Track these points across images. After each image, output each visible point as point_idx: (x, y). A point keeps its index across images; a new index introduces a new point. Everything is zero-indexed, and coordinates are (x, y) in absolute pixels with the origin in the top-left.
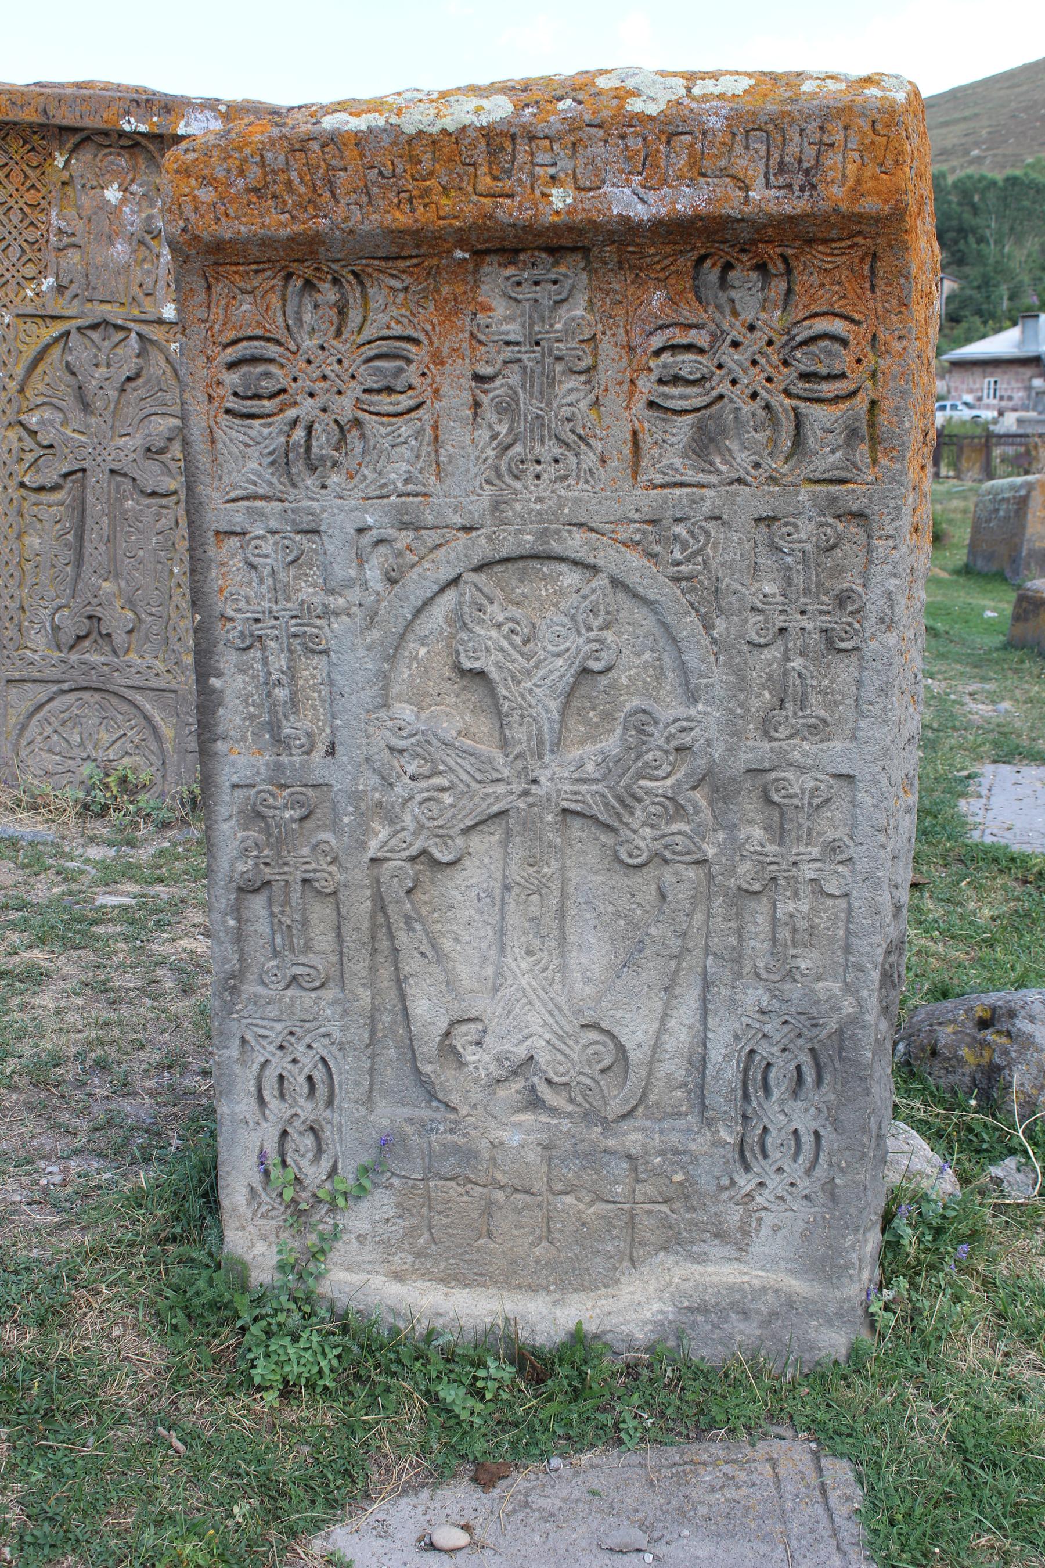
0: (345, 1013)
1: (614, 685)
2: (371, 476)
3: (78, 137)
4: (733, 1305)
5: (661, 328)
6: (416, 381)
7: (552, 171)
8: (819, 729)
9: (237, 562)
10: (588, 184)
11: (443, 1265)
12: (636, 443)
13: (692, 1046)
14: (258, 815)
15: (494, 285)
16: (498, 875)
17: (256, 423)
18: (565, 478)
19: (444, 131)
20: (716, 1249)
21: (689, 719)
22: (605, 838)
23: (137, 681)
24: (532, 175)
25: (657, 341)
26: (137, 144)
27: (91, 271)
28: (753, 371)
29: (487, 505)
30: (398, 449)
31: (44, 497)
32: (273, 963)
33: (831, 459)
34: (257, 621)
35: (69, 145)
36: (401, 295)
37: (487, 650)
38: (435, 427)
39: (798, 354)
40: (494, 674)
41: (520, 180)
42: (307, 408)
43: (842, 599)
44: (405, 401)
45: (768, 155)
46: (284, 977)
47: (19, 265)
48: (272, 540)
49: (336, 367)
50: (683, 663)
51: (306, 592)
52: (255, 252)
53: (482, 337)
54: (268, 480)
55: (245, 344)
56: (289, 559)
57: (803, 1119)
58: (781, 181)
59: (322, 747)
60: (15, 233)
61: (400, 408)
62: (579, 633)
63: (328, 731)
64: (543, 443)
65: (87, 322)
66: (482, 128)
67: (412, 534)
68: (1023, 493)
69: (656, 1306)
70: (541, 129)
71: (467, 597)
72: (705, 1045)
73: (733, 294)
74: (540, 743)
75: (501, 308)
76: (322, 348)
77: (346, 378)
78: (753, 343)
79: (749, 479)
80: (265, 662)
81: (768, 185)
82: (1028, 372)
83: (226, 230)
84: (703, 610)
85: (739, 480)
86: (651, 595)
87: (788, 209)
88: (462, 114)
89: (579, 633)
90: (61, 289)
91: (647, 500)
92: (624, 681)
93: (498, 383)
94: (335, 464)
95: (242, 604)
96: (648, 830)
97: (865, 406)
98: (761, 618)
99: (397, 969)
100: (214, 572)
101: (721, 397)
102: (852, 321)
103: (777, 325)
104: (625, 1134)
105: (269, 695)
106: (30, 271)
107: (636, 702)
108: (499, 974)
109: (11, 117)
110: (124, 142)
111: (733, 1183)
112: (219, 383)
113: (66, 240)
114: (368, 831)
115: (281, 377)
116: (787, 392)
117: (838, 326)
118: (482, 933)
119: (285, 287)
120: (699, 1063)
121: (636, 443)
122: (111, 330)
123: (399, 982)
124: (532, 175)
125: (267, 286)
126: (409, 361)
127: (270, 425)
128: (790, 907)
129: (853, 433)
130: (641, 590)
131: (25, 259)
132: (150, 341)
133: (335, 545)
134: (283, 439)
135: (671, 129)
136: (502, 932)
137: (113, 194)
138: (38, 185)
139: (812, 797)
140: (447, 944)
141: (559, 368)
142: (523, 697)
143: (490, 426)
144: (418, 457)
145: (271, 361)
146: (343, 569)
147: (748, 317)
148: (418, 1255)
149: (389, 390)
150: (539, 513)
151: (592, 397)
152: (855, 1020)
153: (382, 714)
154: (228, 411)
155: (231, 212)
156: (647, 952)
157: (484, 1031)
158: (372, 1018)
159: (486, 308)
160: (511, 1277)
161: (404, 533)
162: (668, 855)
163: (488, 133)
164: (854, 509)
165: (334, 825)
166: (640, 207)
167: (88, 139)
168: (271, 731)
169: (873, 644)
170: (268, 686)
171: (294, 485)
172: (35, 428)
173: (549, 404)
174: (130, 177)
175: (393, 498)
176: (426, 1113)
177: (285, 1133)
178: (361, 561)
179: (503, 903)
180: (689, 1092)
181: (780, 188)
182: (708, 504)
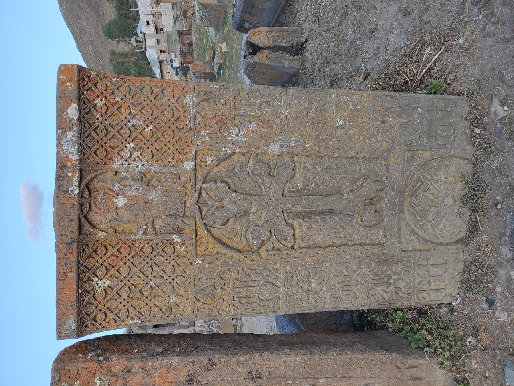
3: (85, 223)
26: (87, 186)
27: (167, 213)
31: (297, 234)
35: (91, 229)
47: (167, 257)
60: (147, 260)
65: (197, 214)
68: (201, 6)
82: (163, 65)
90: (180, 231)
106: (169, 250)
109: (74, 265)
110: (86, 194)
113: (150, 229)
122: (201, 200)
131: (162, 253)
132: (207, 176)
137: (121, 202)
138: (118, 246)
167: (85, 217)
172: (260, 241)
174: (108, 191)
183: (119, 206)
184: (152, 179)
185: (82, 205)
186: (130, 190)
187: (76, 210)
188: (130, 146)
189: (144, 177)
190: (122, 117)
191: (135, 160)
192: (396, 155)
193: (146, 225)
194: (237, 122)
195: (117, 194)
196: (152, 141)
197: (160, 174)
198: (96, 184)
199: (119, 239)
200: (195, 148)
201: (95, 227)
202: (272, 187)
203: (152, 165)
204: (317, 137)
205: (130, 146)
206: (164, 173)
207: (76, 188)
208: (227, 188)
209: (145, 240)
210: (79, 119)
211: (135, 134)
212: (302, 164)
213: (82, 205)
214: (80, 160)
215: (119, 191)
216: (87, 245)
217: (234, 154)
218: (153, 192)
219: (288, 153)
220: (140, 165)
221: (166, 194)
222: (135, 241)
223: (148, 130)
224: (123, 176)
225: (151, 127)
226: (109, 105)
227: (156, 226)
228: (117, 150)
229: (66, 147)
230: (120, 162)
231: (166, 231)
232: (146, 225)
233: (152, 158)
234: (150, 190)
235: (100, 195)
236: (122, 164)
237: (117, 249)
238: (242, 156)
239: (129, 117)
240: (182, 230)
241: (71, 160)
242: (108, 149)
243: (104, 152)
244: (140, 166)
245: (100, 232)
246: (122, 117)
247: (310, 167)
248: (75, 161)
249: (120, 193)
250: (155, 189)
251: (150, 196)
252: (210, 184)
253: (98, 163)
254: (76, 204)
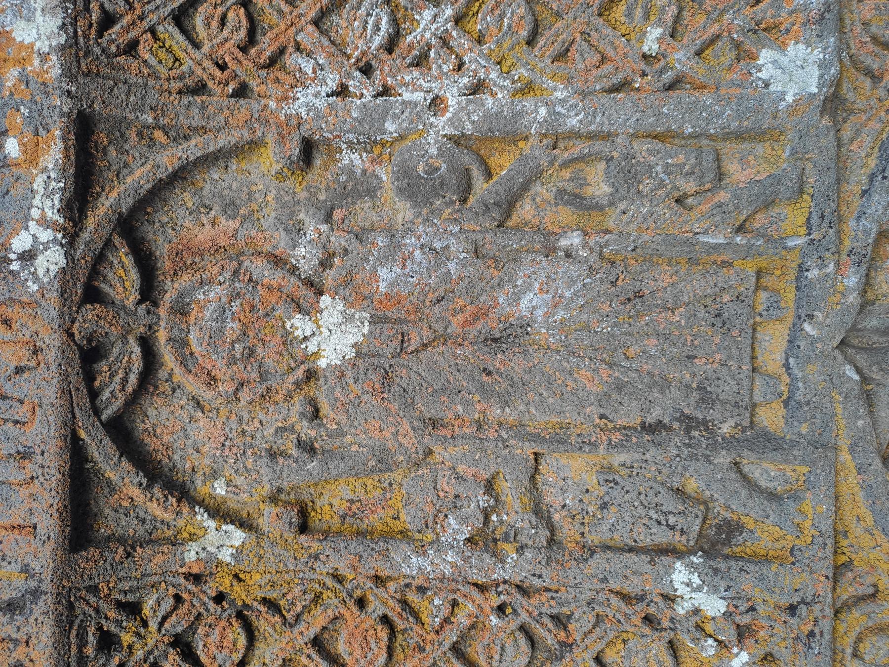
35: (157, 508)
110: (123, 279)
113: (514, 514)
137: (333, 335)
138: (318, 620)
174: (259, 268)
183: (322, 363)
184: (525, 187)
185: (90, 355)
186: (387, 257)
187: (44, 388)
189: (476, 173)
191: (420, 61)
193: (490, 486)
195: (309, 283)
197: (579, 148)
198: (183, 225)
199: (323, 569)
201: (181, 492)
203: (527, 88)
206: (607, 137)
207: (46, 235)
209: (482, 588)
213: (90, 355)
214: (75, 53)
215: (325, 264)
216: (133, 609)
218: (532, 270)
221: (622, 279)
222: (422, 590)
224: (350, 171)
227: (552, 498)
230: (332, 83)
231: (621, 537)
232: (490, 486)
233: (531, 42)
234: (515, 258)
235: (216, 293)
236: (342, 91)
237: (311, 633)
240: (731, 529)
244: (452, 101)
245: (211, 524)
248: (44, 57)
249: (330, 277)
250: (549, 251)
251: (517, 299)
253: (200, 88)
254: (52, 340)
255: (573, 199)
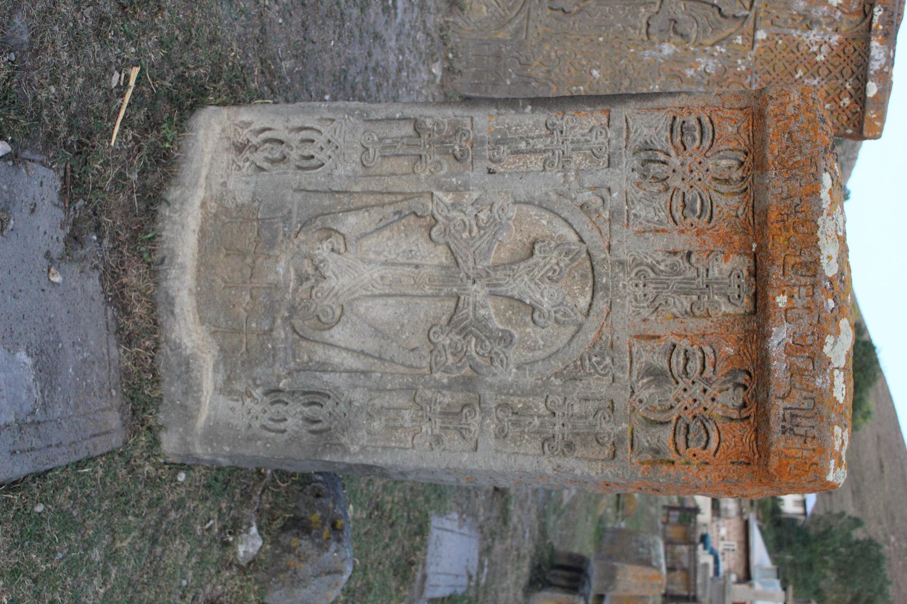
0: (349, 177)
1: (526, 324)
2: (638, 196)
4: (191, 386)
5: (714, 351)
6: (688, 221)
7: (796, 296)
8: (501, 434)
9: (594, 122)
10: (789, 315)
11: (210, 229)
12: (654, 337)
13: (332, 364)
14: (457, 131)
15: (739, 263)
16: (423, 262)
17: (668, 134)
18: (636, 300)
19: (818, 239)
20: (220, 378)
21: (507, 365)
22: (445, 319)
23: (533, 14)
24: (794, 285)
25: (707, 350)
26: (866, 16)
28: (691, 400)
29: (622, 258)
30: (652, 211)
32: (376, 138)
33: (644, 440)
34: (562, 132)
36: (734, 214)
37: (545, 258)
38: (663, 231)
39: (699, 424)
40: (531, 261)
41: (792, 279)
42: (675, 161)
43: (570, 446)
44: (678, 216)
45: (801, 409)
46: (368, 144)
48: (605, 141)
49: (697, 178)
50: (537, 361)
51: (577, 158)
52: (758, 136)
53: (711, 257)
54: (637, 140)
55: (711, 128)
56: (595, 151)
57: (293, 423)
58: (787, 416)
59: (493, 166)
61: (674, 212)
62: (553, 307)
63: (502, 170)
64: (655, 288)
66: (819, 259)
67: (607, 217)
68: (654, 563)
69: (190, 345)
70: (818, 291)
71: (573, 247)
72: (332, 371)
73: (731, 390)
74: (495, 285)
75: (727, 267)
76: (708, 170)
77: (691, 183)
78: (705, 401)
79: (634, 397)
80: (540, 137)
81: (785, 409)
82: (741, 571)
83: (770, 121)
84: (565, 372)
85: (633, 392)
86: (574, 345)
87: (773, 419)
88: (828, 250)
89: (553, 307)
91: (623, 343)
92: (528, 330)
93: (687, 265)
94: (645, 177)
95: (571, 124)
96: (448, 342)
97: (672, 458)
98: (561, 402)
99: (373, 206)
100: (588, 109)
101: (677, 383)
102: (716, 452)
103: (714, 413)
104: (284, 329)
105: (521, 138)
107: (517, 336)
108: (370, 262)
110: (867, 8)
111: (258, 386)
112: (690, 113)
114: (448, 191)
115: (692, 147)
116: (679, 418)
117: (713, 445)
118: (392, 252)
119: (740, 151)
120: (324, 367)
121: (654, 337)
123: (366, 207)
124: (794, 285)
125: (741, 141)
126: (699, 217)
127: (667, 141)
128: (407, 417)
129: (657, 451)
130: (575, 340)
133: (602, 175)
134: (659, 148)
135: (816, 359)
136: (393, 264)
139: (466, 429)
140: (387, 233)
141: (695, 298)
142: (520, 276)
143: (664, 260)
144: (648, 221)
145: (701, 142)
146: (588, 181)
147: (719, 398)
148: (215, 215)
149: (685, 206)
150: (617, 286)
151: (678, 314)
152: (346, 451)
153: (511, 200)
154: (674, 118)
155: (780, 124)
156: (383, 341)
157: (339, 253)
158: (346, 192)
159: (726, 259)
160: (204, 266)
161: (607, 213)
162: (435, 353)
163: (817, 262)
164: (617, 452)
165: (453, 174)
166: (776, 342)
168: (502, 139)
169: (546, 462)
170: (526, 139)
171: (634, 154)
173: (675, 292)
174: (846, 11)
175: (626, 207)
176: (294, 221)
177: (282, 142)
178: (594, 188)
179: (409, 265)
180: (307, 363)
181: (784, 415)
182: (621, 376)
186: (824, 13)
188: (820, 58)
190: (826, 87)
191: (816, 42)
192: (535, 35)
194: (707, 78)
196: (797, 62)
198: (857, 18)
200: (753, 53)
202: (674, 8)
203: (800, 36)
204: (621, 59)
205: (820, 58)
208: (723, 10)
210: (866, 82)
211: (814, 69)
212: (638, 32)
214: (869, 40)
217: (713, 45)
219: (653, 44)
220: (811, 37)
223: (800, 73)
225: (797, 76)
226: (837, 99)
228: (834, 53)
229: (882, 55)
238: (702, 42)
239: (819, 87)
241: (878, 41)
242: (842, 55)
243: (846, 51)
246: (826, 87)
247: (630, 29)
252: (740, 14)
253: (853, 39)
255: (793, 20)
